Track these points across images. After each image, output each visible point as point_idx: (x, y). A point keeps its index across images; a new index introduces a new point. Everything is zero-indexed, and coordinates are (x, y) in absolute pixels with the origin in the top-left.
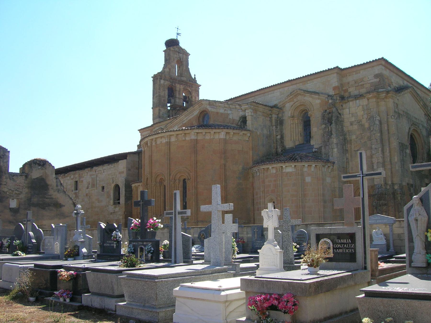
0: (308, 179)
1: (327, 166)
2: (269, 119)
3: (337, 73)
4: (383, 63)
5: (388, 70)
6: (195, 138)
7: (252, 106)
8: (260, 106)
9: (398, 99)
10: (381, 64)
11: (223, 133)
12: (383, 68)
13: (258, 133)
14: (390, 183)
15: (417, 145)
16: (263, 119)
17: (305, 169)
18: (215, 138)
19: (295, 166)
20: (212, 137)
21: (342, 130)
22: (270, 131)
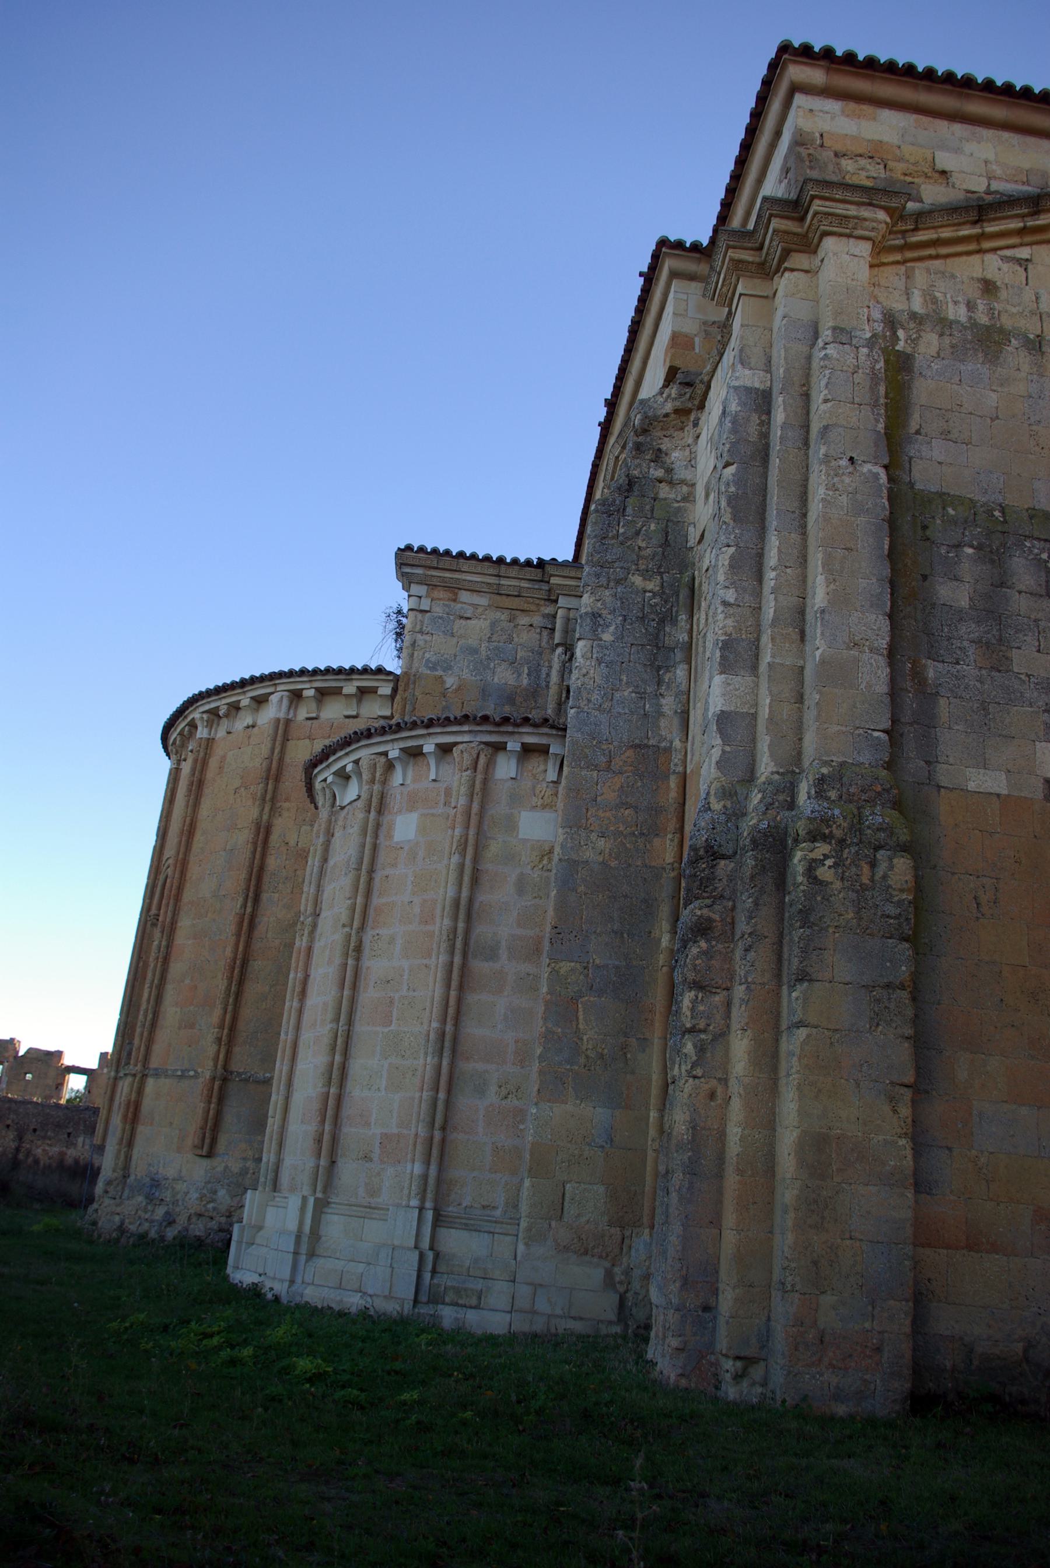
0: (405, 827)
1: (513, 745)
2: (537, 620)
3: (674, 275)
4: (816, 75)
5: (886, 114)
6: (205, 735)
7: (419, 571)
8: (465, 566)
9: (1024, 263)
10: (795, 89)
11: (274, 698)
12: (833, 106)
13: (450, 681)
14: (766, 767)
16: (493, 625)
17: (397, 777)
18: (260, 722)
19: (356, 762)
20: (249, 721)
21: (666, 543)
22: (535, 671)
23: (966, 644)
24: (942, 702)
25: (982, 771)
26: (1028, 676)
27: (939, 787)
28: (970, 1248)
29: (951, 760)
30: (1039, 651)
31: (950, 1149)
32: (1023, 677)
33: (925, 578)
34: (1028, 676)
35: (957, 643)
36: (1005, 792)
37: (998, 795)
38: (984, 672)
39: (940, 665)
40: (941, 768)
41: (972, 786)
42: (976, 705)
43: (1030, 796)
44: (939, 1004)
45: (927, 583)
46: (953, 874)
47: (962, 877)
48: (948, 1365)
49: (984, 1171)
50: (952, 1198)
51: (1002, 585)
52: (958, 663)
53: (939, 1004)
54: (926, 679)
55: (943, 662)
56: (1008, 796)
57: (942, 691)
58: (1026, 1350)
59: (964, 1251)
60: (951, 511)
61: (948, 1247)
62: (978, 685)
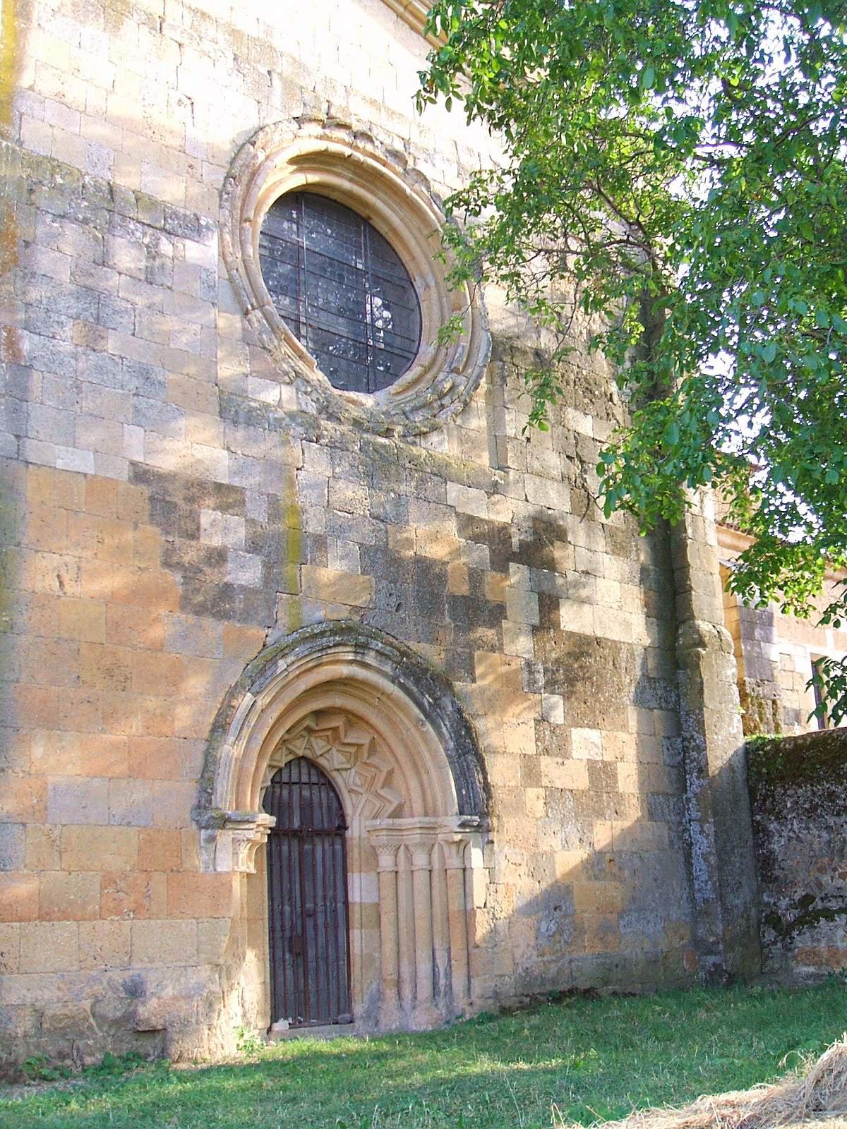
15: (418, 283)
23: (63, 318)
24: (36, 376)
25: (71, 449)
26: (122, 358)
27: (27, 463)
28: (41, 918)
29: (41, 436)
30: (133, 335)
31: (24, 825)
32: (116, 358)
33: (27, 244)
34: (122, 358)
35: (55, 317)
36: (93, 472)
37: (85, 475)
38: (80, 349)
39: (36, 338)
40: (30, 444)
41: (60, 464)
42: (70, 382)
43: (115, 477)
44: (18, 681)
45: (28, 251)
46: (37, 551)
47: (45, 555)
48: (20, 1032)
49: (58, 842)
50: (25, 871)
51: (104, 264)
52: (54, 337)
53: (18, 681)
54: (20, 350)
55: (39, 334)
56: (95, 476)
57: (36, 364)
58: (93, 1006)
59: (37, 922)
60: (60, 180)
61: (20, 921)
62: (73, 362)
